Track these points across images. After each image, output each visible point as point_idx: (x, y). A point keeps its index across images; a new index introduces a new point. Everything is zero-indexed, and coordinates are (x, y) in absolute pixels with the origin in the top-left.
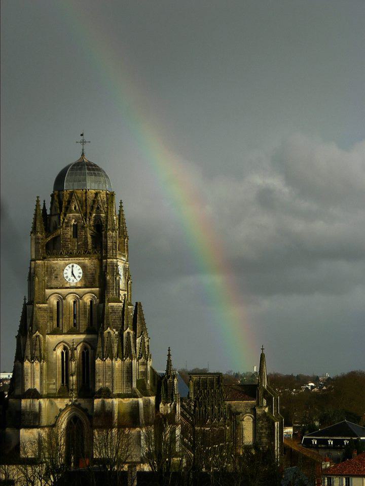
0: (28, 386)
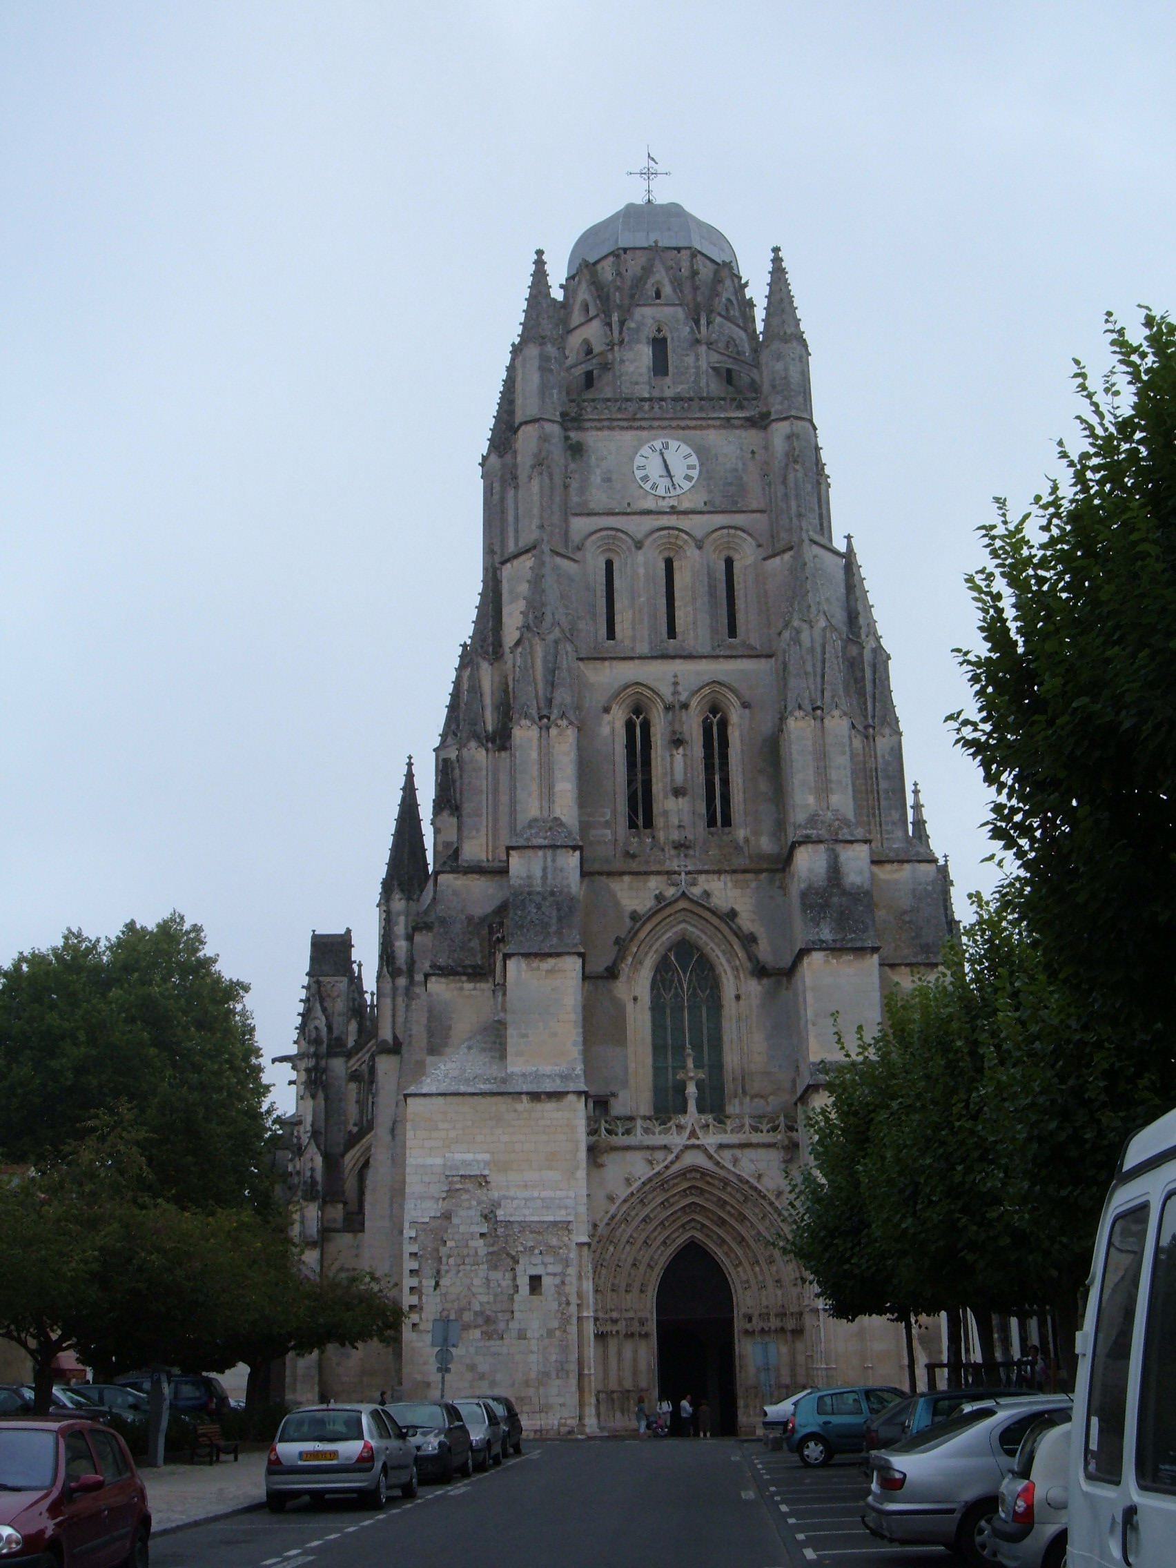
0: (531, 808)
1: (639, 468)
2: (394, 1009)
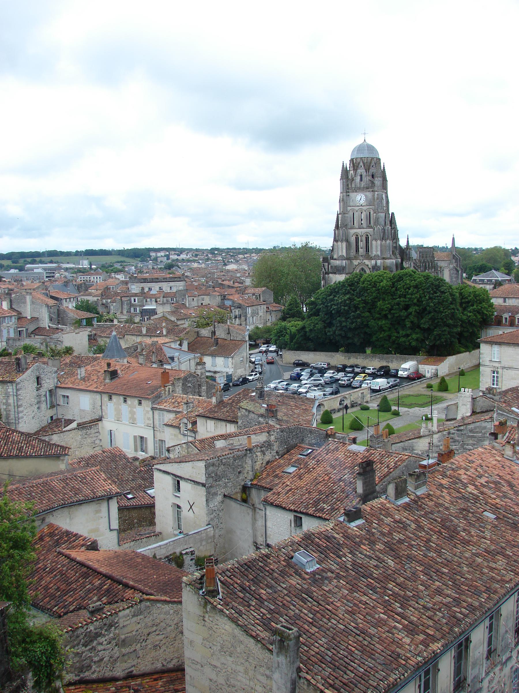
0: (340, 254)
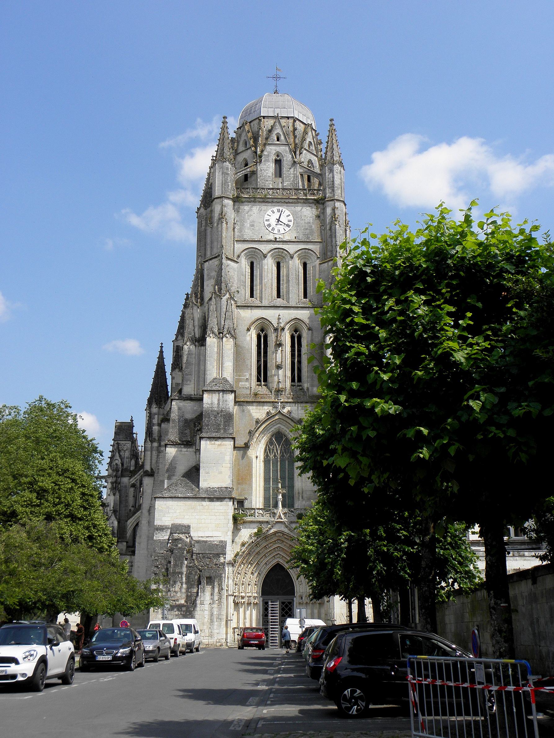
1: (267, 220)
2: (151, 457)
